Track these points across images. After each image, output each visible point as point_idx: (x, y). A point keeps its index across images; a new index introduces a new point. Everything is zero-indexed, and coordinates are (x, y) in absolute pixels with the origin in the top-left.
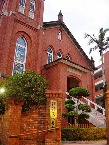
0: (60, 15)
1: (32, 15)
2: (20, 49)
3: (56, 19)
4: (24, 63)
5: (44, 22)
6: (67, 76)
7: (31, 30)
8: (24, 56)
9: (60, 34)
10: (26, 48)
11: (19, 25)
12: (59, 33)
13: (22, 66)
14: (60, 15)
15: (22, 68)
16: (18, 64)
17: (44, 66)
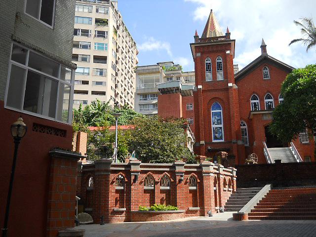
0: (264, 47)
1: (220, 77)
2: (215, 114)
3: (258, 53)
4: (222, 126)
5: (235, 73)
6: (264, 126)
7: (221, 92)
8: (220, 119)
9: (267, 71)
10: (221, 111)
11: (209, 94)
12: (267, 69)
13: (221, 128)
14: (264, 47)
15: (220, 130)
16: (216, 128)
17: (249, 118)
